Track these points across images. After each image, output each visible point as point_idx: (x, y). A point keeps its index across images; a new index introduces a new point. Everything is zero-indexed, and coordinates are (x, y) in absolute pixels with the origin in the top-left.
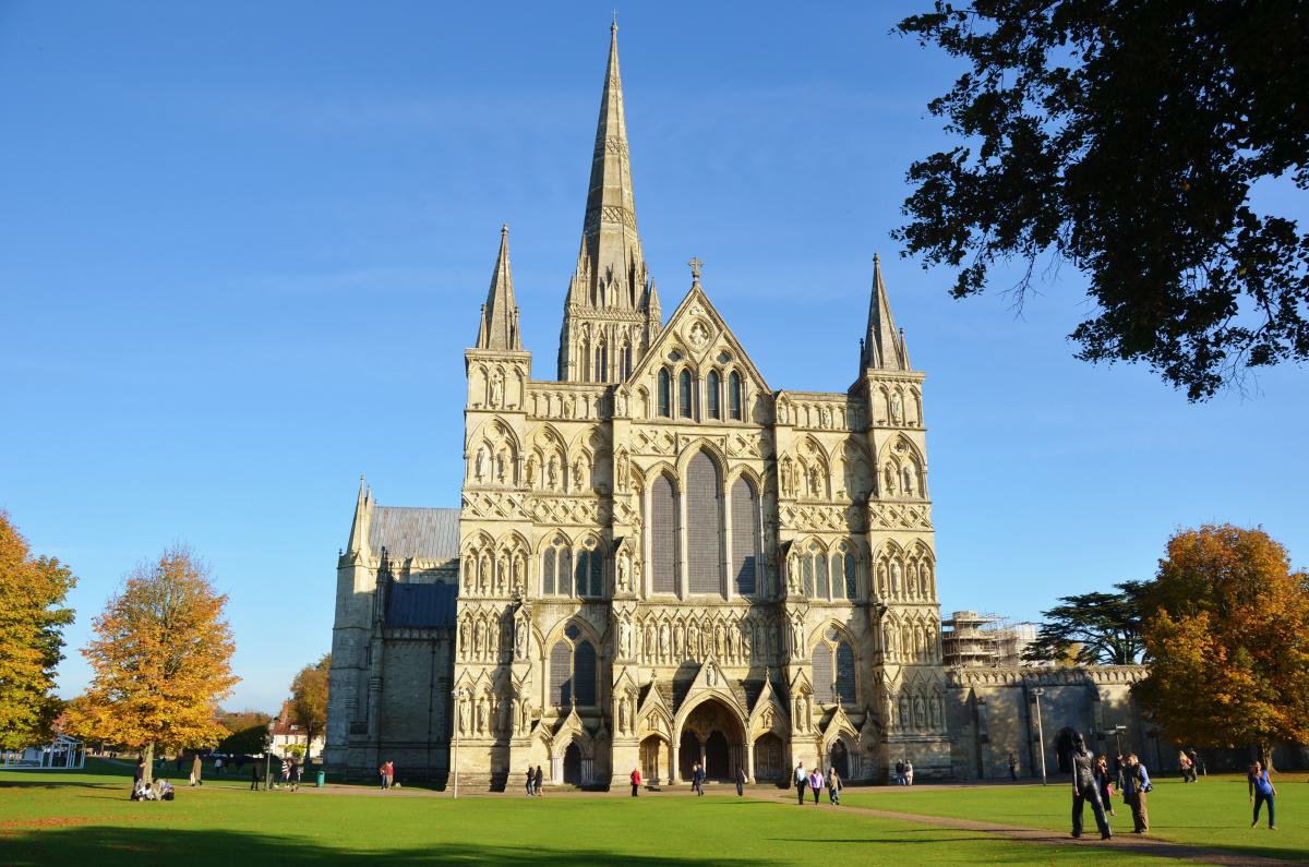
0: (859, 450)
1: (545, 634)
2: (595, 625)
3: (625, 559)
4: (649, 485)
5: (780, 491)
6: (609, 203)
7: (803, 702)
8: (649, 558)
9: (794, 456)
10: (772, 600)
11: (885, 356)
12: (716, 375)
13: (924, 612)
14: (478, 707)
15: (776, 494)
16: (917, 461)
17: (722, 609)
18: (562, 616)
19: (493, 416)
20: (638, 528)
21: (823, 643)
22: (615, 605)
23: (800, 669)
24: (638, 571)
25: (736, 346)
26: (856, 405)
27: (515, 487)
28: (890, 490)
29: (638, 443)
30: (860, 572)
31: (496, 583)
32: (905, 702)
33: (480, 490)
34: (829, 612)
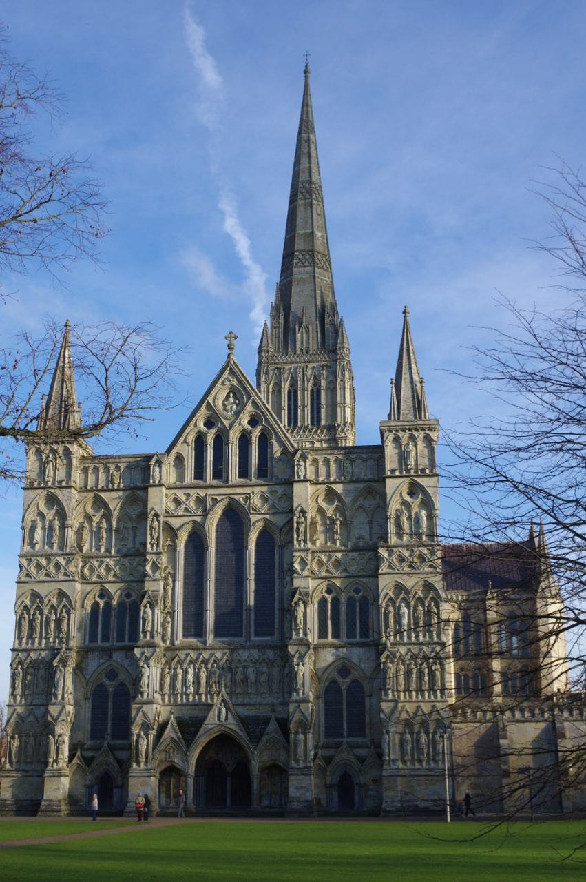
0: (378, 496)
2: (129, 668)
3: (149, 611)
6: (302, 248)
7: (301, 736)
12: (244, 439)
14: (25, 742)
17: (241, 652)
19: (44, 492)
20: (170, 580)
21: (334, 682)
24: (169, 619)
27: (61, 552)
28: (400, 536)
31: (44, 635)
32: (408, 737)
33: (33, 556)
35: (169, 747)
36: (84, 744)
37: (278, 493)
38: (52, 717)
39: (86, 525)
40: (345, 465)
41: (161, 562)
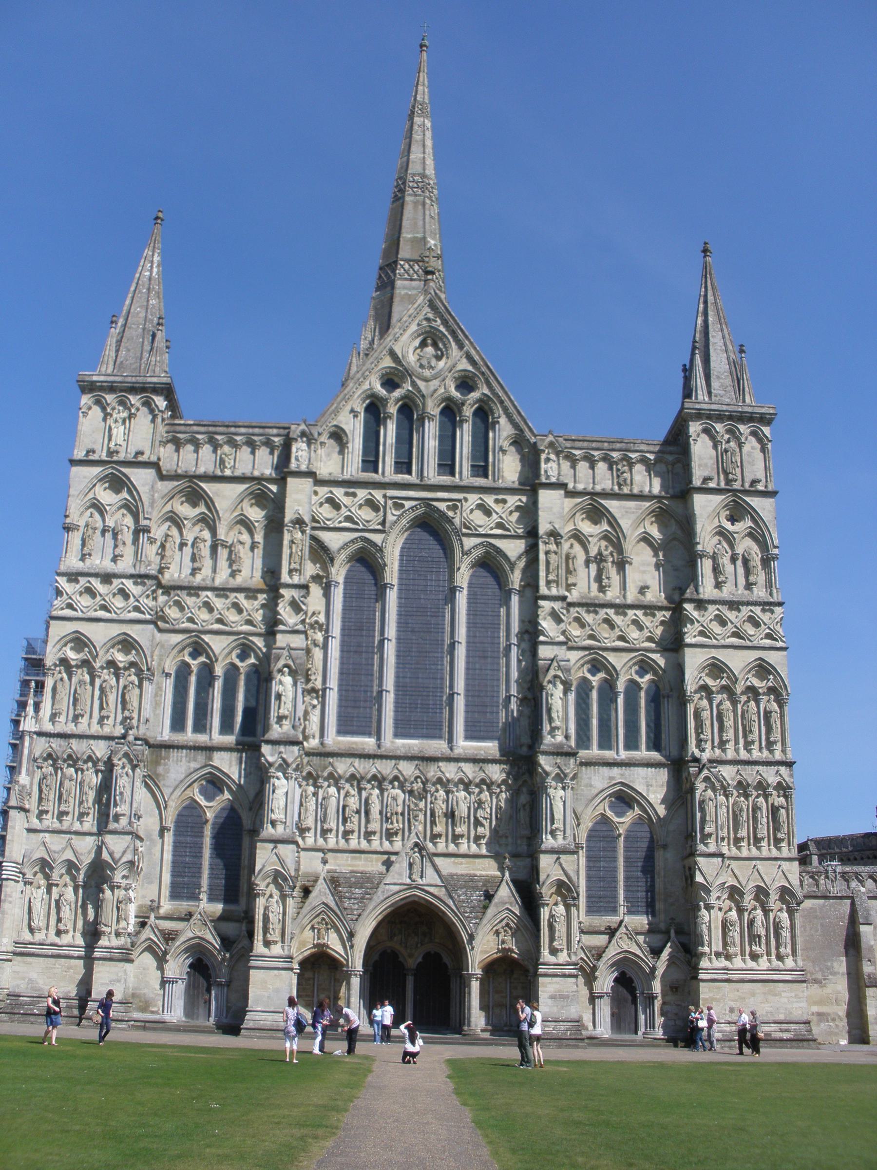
0: (673, 521)
1: (167, 791)
3: (288, 680)
4: (339, 573)
5: (542, 583)
8: (333, 682)
9: (566, 529)
10: (524, 751)
11: (715, 384)
13: (771, 776)
15: (536, 587)
16: (758, 536)
18: (194, 765)
21: (604, 820)
22: (266, 749)
23: (558, 858)
25: (484, 369)
26: (670, 458)
28: (718, 585)
29: (326, 512)
30: (669, 710)
34: (616, 771)
35: (318, 919)
36: (159, 907)
37: (508, 505)
38: (111, 854)
39: (175, 532)
40: (620, 467)
41: (306, 601)
